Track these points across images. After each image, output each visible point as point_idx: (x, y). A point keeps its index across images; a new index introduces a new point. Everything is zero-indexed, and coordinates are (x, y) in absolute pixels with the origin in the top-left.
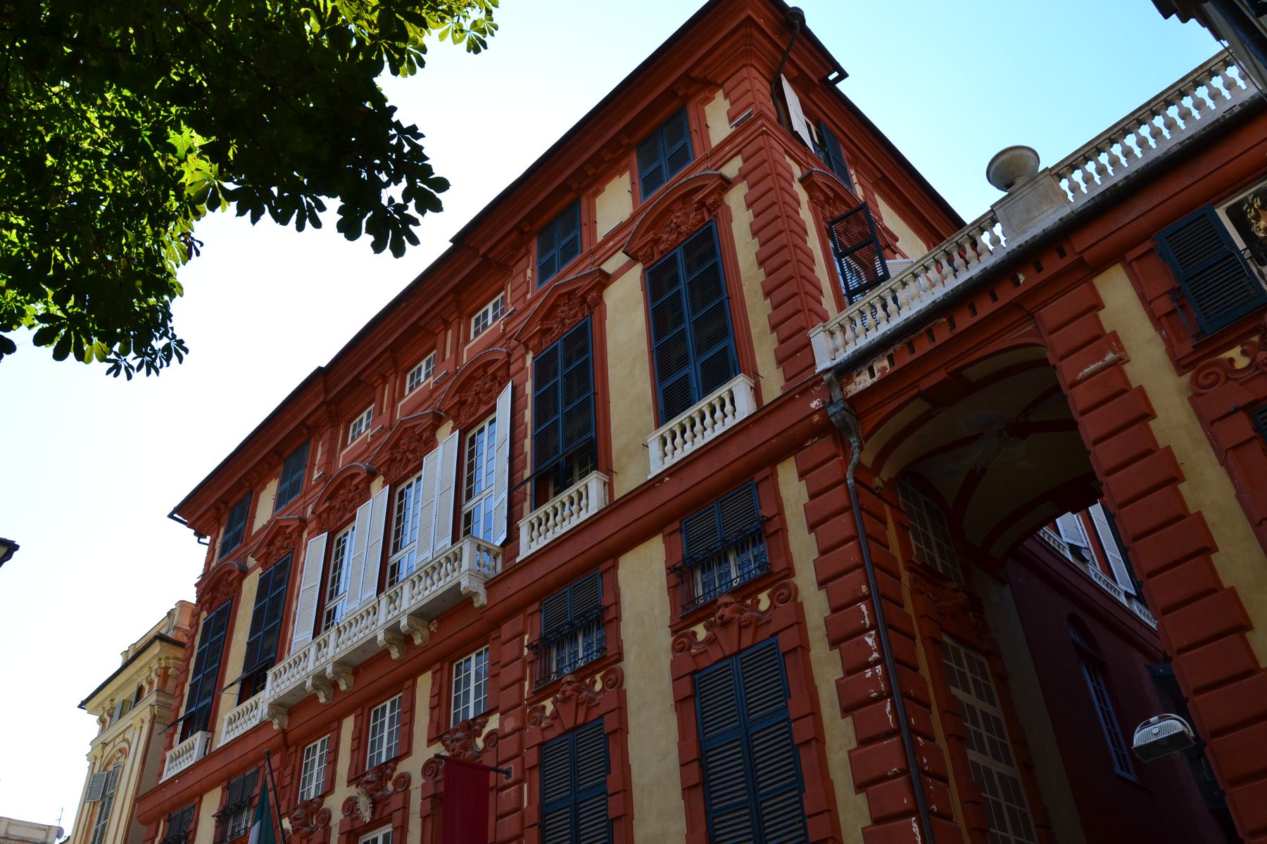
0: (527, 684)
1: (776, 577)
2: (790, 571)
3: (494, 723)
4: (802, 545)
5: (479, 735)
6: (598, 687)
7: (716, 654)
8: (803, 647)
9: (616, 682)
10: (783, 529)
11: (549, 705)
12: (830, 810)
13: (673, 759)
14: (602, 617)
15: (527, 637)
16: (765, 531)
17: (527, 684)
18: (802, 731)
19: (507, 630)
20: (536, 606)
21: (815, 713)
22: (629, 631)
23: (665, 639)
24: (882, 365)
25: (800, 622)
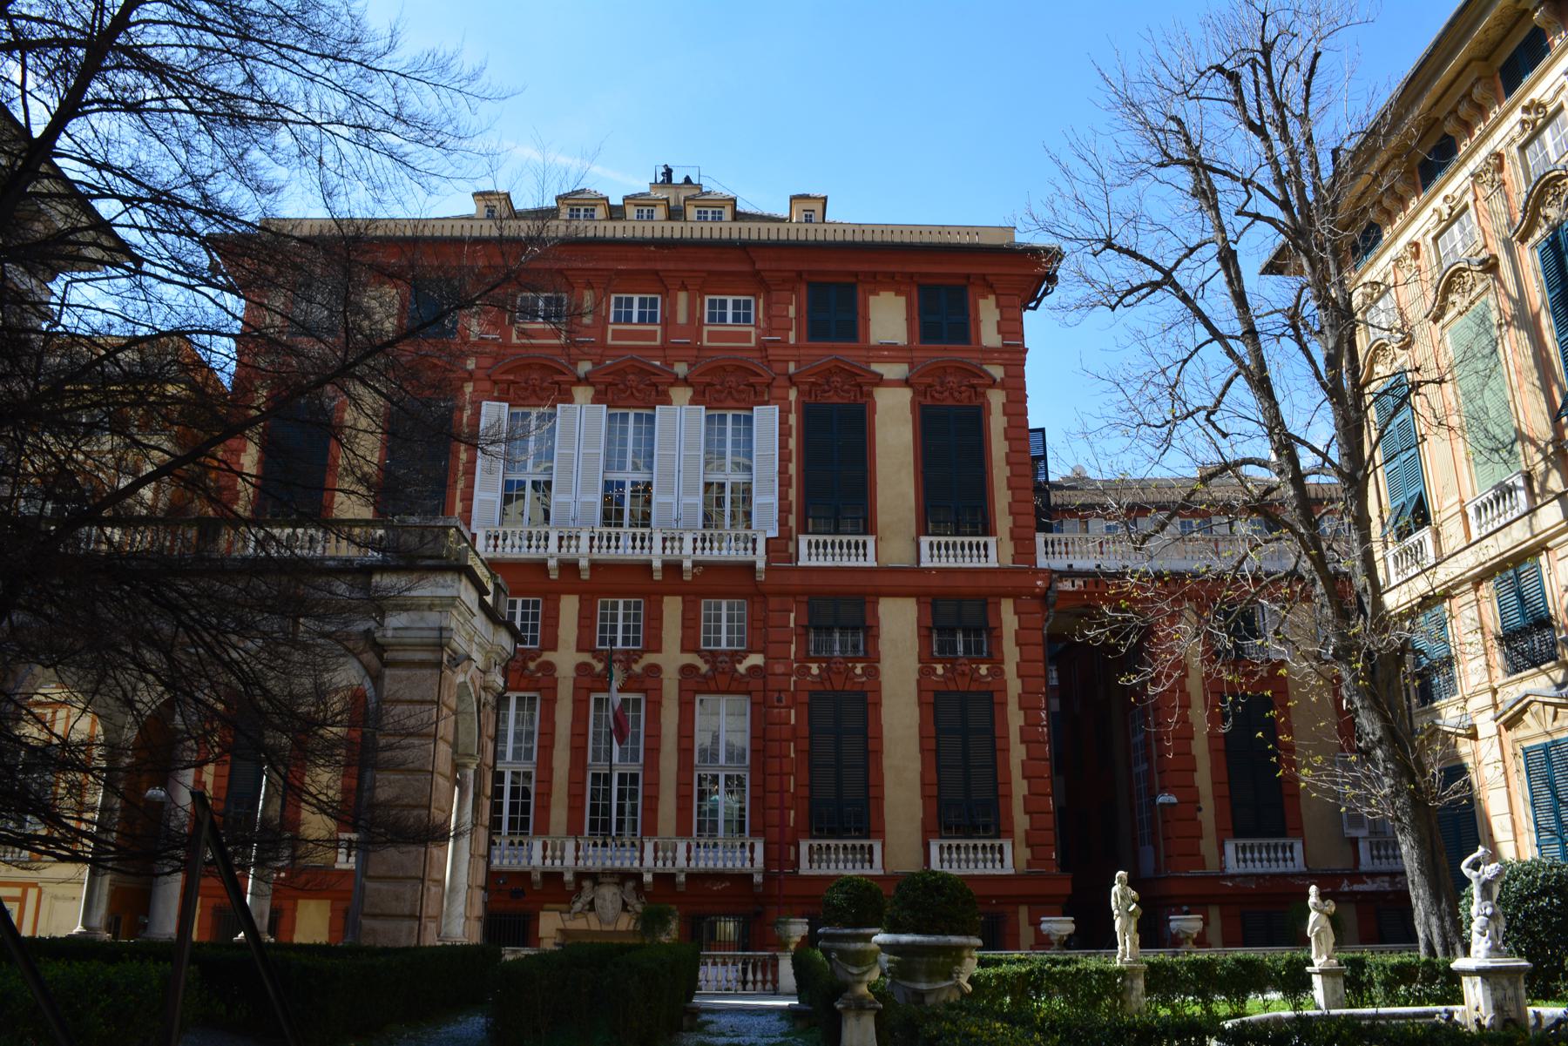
0: (793, 647)
1: (996, 662)
2: (1002, 662)
3: (756, 659)
4: (1011, 653)
5: (740, 662)
6: (858, 671)
7: (952, 687)
8: (1004, 704)
9: (873, 672)
10: (1000, 637)
11: (815, 669)
12: (1009, 783)
13: (915, 731)
14: (868, 629)
15: (792, 615)
16: (995, 634)
17: (793, 647)
18: (999, 744)
19: (774, 602)
20: (805, 599)
21: (1007, 738)
22: (884, 646)
23: (913, 664)
24: (1079, 582)
25: (1004, 691)
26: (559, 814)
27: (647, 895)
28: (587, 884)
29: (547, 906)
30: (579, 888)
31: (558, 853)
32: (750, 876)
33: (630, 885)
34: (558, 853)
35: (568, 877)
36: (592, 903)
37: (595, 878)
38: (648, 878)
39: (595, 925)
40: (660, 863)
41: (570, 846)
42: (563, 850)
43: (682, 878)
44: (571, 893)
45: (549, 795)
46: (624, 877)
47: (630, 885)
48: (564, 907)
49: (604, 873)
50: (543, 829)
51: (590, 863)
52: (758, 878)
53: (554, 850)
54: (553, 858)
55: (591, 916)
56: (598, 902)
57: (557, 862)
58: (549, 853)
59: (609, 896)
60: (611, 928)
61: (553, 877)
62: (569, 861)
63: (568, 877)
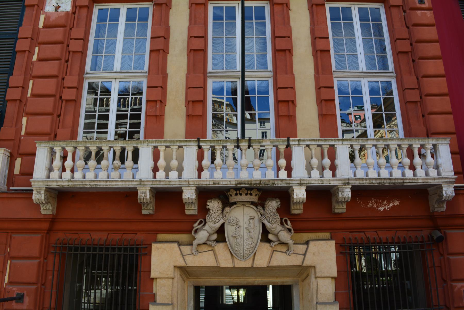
26: (175, 120)
27: (295, 219)
28: (214, 205)
29: (161, 236)
30: (204, 210)
31: (174, 163)
32: (439, 187)
33: (273, 205)
34: (174, 163)
35: (189, 195)
36: (221, 231)
37: (224, 195)
38: (300, 194)
39: (225, 261)
40: (316, 174)
41: (191, 151)
42: (181, 160)
43: (347, 193)
44: (193, 219)
45: (163, 102)
46: (264, 194)
47: (273, 205)
48: (183, 237)
49: (238, 190)
50: (156, 132)
51: (218, 175)
52: (448, 191)
53: (168, 159)
54: (168, 170)
55: (220, 247)
56: (229, 230)
57: (173, 175)
58: (161, 163)
59: (243, 220)
60: (247, 264)
61: (167, 197)
62: (190, 173)
63: (189, 195)
